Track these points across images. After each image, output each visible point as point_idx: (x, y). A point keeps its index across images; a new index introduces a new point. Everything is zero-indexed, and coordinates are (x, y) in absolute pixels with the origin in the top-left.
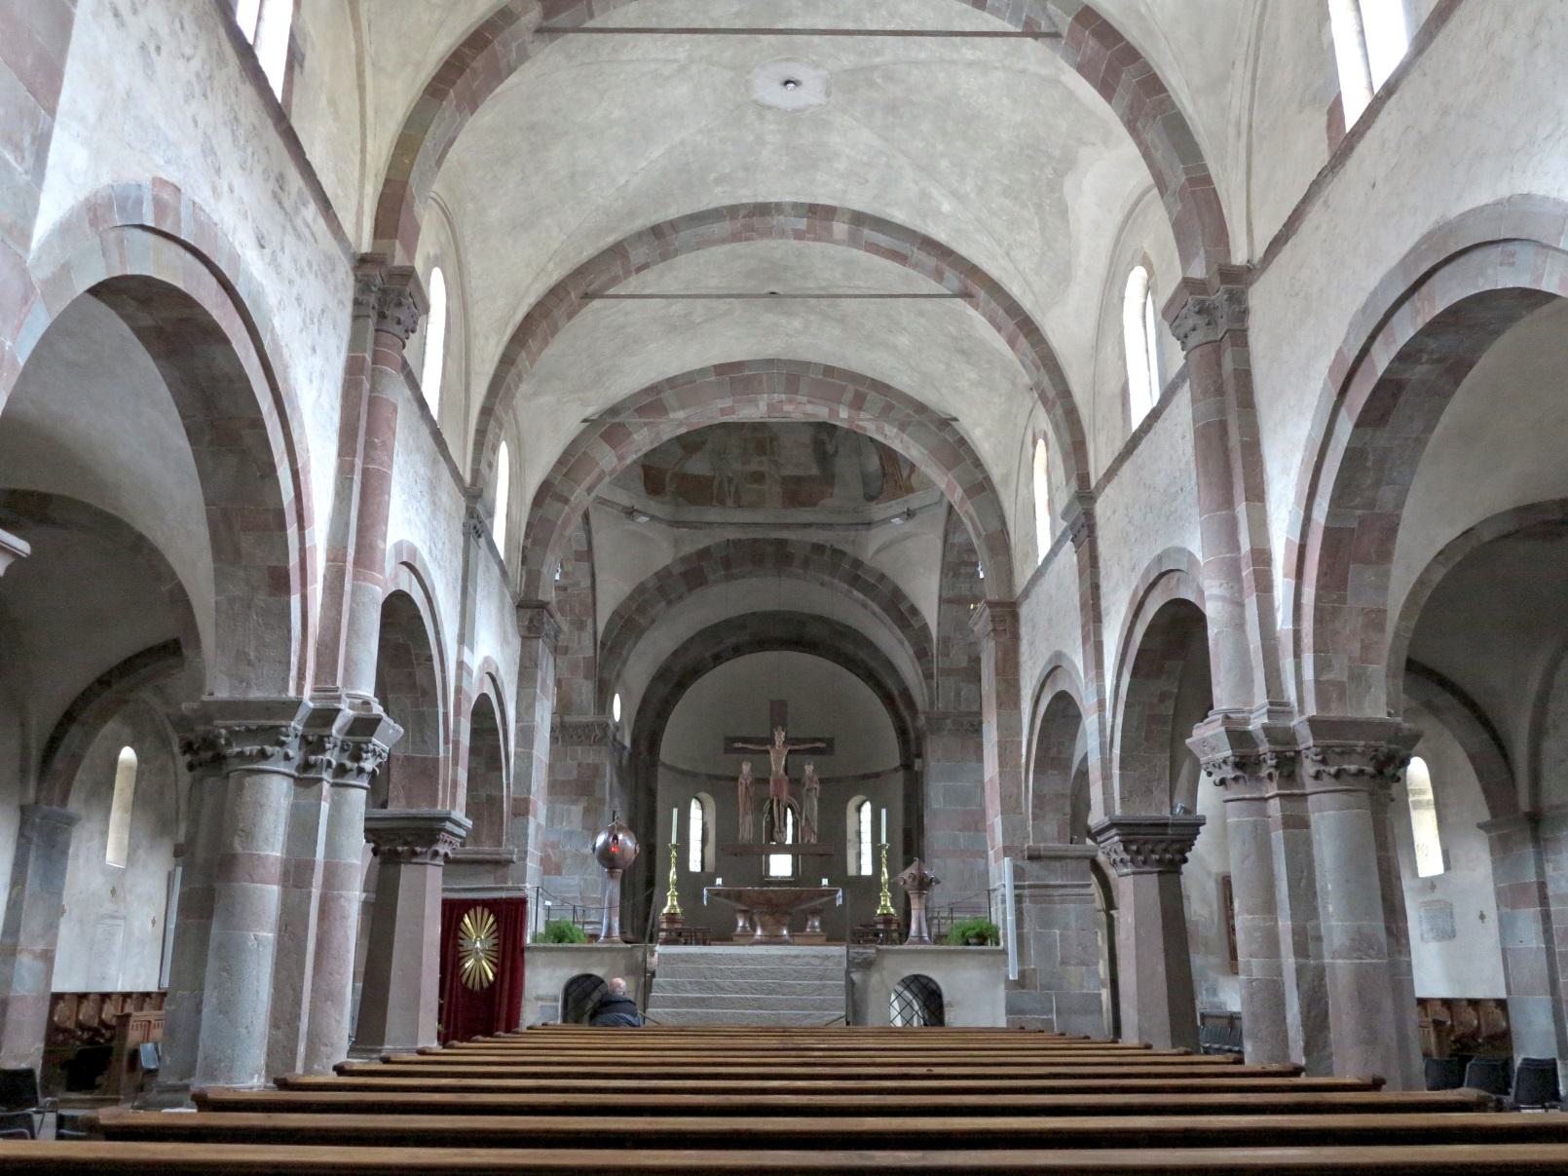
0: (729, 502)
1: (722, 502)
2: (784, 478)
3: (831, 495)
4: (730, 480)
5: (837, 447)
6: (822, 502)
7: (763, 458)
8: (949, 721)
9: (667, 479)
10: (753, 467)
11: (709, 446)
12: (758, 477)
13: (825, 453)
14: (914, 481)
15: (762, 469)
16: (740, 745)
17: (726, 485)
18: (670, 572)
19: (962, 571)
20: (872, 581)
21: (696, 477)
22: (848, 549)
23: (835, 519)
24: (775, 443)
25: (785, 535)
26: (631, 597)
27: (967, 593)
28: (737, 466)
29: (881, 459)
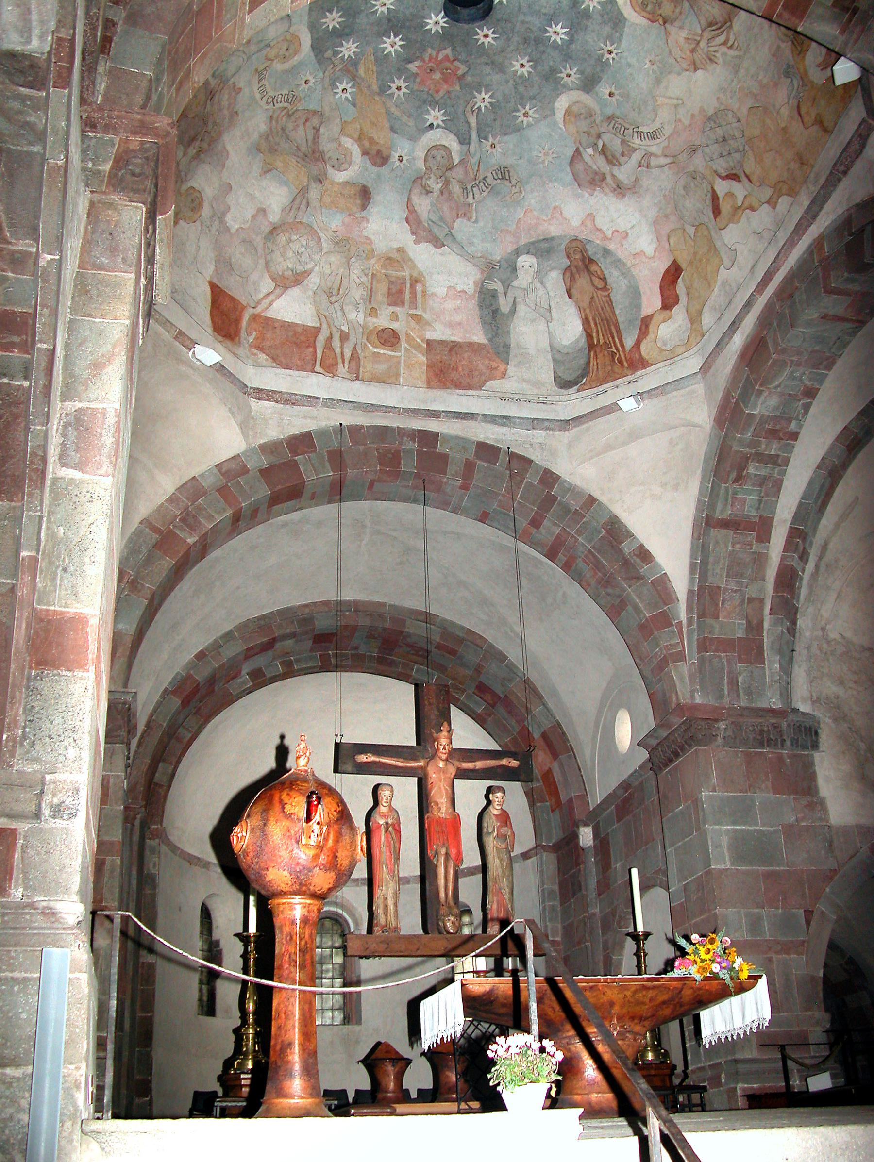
0: (342, 370)
1: (330, 369)
2: (429, 342)
3: (503, 375)
4: (344, 337)
5: (514, 303)
6: (488, 384)
7: (397, 309)
8: (722, 725)
9: (244, 323)
10: (383, 321)
11: (314, 280)
12: (390, 338)
13: (495, 312)
14: (645, 349)
15: (395, 326)
16: (372, 758)
17: (336, 343)
18: (244, 470)
19: (751, 470)
20: (574, 505)
21: (288, 326)
22: (535, 456)
23: (512, 411)
24: (419, 288)
25: (432, 426)
26: (172, 500)
27: (754, 513)
28: (357, 316)
29: (586, 322)
